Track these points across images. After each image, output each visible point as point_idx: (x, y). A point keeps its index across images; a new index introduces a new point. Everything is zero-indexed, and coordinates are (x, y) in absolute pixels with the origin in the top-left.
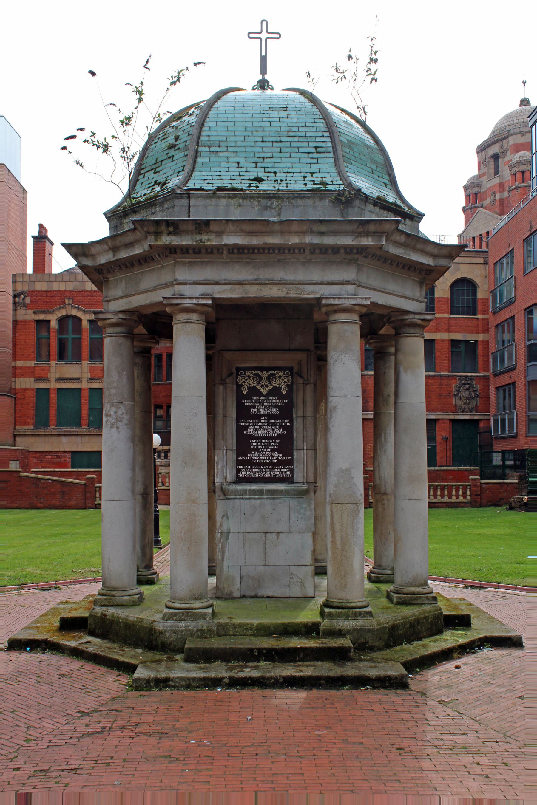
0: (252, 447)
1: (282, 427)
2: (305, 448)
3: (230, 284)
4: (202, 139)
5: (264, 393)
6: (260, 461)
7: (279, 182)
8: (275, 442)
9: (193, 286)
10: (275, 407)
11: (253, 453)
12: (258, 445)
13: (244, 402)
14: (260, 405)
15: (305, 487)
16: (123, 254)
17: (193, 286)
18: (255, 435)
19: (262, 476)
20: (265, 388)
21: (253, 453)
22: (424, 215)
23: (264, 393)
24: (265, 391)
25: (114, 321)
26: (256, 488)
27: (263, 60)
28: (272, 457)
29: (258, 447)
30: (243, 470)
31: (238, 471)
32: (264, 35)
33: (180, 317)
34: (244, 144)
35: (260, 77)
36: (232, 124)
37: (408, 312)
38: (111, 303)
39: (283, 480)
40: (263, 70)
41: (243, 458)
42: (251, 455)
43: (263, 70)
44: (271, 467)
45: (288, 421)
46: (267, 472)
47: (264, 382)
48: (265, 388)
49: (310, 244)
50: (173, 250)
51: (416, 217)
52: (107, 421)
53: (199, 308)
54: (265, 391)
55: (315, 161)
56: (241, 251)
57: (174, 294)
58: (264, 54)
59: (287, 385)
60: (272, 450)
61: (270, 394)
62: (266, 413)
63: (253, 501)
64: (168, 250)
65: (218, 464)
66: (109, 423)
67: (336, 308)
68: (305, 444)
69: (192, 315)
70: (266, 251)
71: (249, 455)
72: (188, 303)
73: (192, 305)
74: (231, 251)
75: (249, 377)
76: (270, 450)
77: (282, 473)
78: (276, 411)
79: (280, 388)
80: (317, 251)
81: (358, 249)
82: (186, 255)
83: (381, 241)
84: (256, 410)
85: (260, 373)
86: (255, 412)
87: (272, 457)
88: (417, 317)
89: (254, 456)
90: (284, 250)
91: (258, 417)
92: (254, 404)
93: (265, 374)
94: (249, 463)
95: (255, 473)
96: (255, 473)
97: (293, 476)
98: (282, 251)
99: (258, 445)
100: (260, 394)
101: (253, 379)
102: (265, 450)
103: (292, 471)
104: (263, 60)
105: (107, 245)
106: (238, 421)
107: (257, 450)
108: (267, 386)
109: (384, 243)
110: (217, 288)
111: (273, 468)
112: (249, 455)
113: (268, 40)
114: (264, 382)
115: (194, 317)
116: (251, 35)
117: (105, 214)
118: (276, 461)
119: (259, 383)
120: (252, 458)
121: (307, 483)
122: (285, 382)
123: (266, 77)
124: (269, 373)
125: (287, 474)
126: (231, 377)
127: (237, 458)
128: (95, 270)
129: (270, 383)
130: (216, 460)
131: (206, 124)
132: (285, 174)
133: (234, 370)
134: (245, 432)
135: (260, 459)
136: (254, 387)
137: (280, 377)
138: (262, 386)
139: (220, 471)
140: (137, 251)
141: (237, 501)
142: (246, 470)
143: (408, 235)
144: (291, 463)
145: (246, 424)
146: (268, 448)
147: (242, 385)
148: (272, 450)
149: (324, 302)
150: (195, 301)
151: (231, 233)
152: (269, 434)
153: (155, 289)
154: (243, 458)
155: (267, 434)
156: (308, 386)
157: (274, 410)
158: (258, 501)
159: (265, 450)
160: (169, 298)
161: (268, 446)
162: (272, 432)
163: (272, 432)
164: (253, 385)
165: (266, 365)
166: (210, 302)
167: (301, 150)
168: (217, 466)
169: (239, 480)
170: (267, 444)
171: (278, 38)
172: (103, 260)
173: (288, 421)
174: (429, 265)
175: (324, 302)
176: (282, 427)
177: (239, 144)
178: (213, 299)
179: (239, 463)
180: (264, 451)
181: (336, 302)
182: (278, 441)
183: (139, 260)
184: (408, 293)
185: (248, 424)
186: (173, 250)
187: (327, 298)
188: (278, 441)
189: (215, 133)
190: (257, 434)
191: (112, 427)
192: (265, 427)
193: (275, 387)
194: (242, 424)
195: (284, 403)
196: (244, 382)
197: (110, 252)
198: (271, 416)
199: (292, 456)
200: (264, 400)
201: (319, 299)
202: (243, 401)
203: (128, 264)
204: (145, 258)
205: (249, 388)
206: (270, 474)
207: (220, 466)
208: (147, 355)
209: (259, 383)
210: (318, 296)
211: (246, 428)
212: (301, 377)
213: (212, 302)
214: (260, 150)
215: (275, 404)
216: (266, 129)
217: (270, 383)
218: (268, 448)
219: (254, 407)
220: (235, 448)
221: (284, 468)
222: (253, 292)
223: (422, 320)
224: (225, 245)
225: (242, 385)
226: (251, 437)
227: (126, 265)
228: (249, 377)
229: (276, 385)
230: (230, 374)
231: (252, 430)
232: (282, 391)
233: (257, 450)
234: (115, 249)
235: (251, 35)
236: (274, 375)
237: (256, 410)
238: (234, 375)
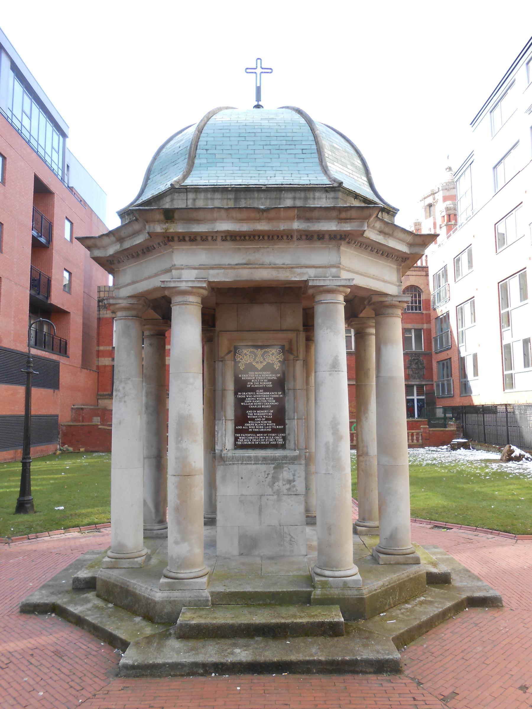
0: (249, 417)
1: (275, 398)
2: (296, 418)
3: (223, 268)
4: (199, 143)
5: (259, 369)
6: (255, 430)
7: (268, 178)
8: (269, 412)
9: (189, 270)
10: (269, 381)
11: (250, 422)
12: (254, 415)
13: (242, 377)
14: (255, 379)
15: (297, 453)
16: (127, 244)
17: (189, 270)
18: (252, 407)
19: (257, 443)
20: (259, 364)
21: (250, 422)
22: (399, 210)
23: (259, 369)
24: (259, 366)
25: (122, 305)
26: (252, 455)
27: (258, 89)
28: (266, 426)
29: (254, 417)
30: (240, 438)
31: (236, 439)
32: (259, 70)
33: (176, 299)
34: (238, 147)
35: (256, 103)
36: (228, 131)
37: (386, 295)
38: (121, 290)
39: (276, 447)
40: (258, 98)
41: (241, 427)
42: (248, 425)
43: (258, 98)
44: (266, 435)
45: (280, 393)
46: (263, 440)
47: (259, 358)
48: (259, 364)
49: (298, 231)
50: (170, 238)
51: (391, 211)
52: (116, 396)
53: (195, 290)
54: (259, 366)
55: (302, 160)
56: (233, 238)
57: (172, 278)
58: (258, 85)
59: (279, 361)
60: (267, 419)
61: (264, 369)
62: (261, 386)
63: (249, 466)
64: (167, 238)
65: (218, 433)
66: (118, 397)
67: (321, 289)
68: (296, 414)
69: (188, 297)
70: (257, 238)
71: (246, 425)
72: (183, 286)
73: (190, 289)
74: (224, 238)
75: (246, 355)
76: (264, 419)
77: (276, 440)
78: (270, 385)
79: (273, 364)
80: (304, 237)
81: (341, 236)
82: (183, 243)
83: (362, 226)
84: (252, 383)
85: (256, 351)
86: (251, 385)
87: (266, 426)
88: (395, 299)
89: (250, 425)
90: (272, 236)
91: (253, 390)
92: (250, 378)
93: (259, 352)
94: (246, 431)
95: (252, 441)
96: (252, 441)
97: (285, 443)
98: (271, 237)
99: (254, 415)
100: (256, 370)
101: (249, 356)
102: (260, 419)
103: (284, 438)
104: (258, 89)
105: (114, 236)
106: (236, 394)
107: (253, 420)
108: (261, 362)
109: (366, 228)
110: (211, 272)
111: (267, 436)
112: (246, 425)
113: (262, 74)
114: (259, 358)
115: (191, 298)
116: (248, 71)
117: (118, 213)
118: (270, 430)
119: (255, 359)
120: (248, 426)
121: (299, 449)
122: (278, 359)
123: (260, 103)
124: (263, 351)
125: (280, 441)
126: (230, 355)
127: (235, 427)
128: (107, 261)
129: (264, 359)
130: (216, 429)
131: (203, 131)
132: (274, 172)
133: (232, 349)
134: (242, 404)
135: (256, 428)
136: (251, 364)
137: (273, 354)
138: (257, 362)
139: (220, 439)
140: (139, 240)
141: (235, 466)
142: (243, 438)
143: (386, 223)
144: (283, 431)
145: (243, 396)
146: (263, 418)
147: (239, 362)
148: (267, 419)
149: (310, 284)
150: (190, 284)
151: (221, 219)
152: (263, 405)
153: (156, 275)
154: (241, 427)
155: (261, 405)
156: (298, 362)
157: (268, 383)
158: (254, 467)
159: (260, 419)
160: (167, 281)
161: (263, 416)
162: (266, 404)
163: (266, 404)
164: (249, 361)
165: (260, 344)
166: (205, 285)
167: (289, 152)
168: (217, 435)
169: (237, 447)
170: (262, 414)
171: (271, 73)
172: (111, 251)
173: (280, 393)
174: (405, 253)
175: (310, 284)
176: (275, 398)
177: (234, 147)
178: (209, 283)
179: (237, 431)
180: (260, 421)
181: (322, 283)
182: (272, 411)
183: (143, 250)
184: (387, 278)
185: (244, 396)
186: (170, 238)
187: (313, 280)
188: (272, 411)
189: (212, 139)
190: (253, 405)
191: (120, 401)
192: (260, 399)
193: (268, 363)
194: (240, 396)
195: (277, 377)
196: (241, 359)
197: (118, 243)
198: (266, 389)
199: (284, 424)
200: (259, 375)
201: (306, 282)
202: (240, 376)
203: (134, 254)
204: (148, 248)
205: (246, 364)
206: (265, 441)
207: (219, 435)
208: (162, 337)
209: (255, 359)
210: (305, 278)
211: (243, 400)
212: (292, 354)
213: (208, 285)
214: (252, 152)
215: (269, 378)
216: (257, 134)
217: (264, 359)
218: (263, 418)
219: (250, 381)
220: (233, 418)
221: (277, 436)
222: (245, 275)
223: (400, 301)
224: (217, 232)
225: (239, 362)
226: (247, 408)
227: (132, 254)
228: (246, 355)
229: (270, 361)
230: (229, 352)
231: (248, 401)
232: (275, 366)
233: (253, 420)
234: (121, 240)
235: (248, 71)
236: (268, 352)
237: (252, 383)
238: (233, 353)
